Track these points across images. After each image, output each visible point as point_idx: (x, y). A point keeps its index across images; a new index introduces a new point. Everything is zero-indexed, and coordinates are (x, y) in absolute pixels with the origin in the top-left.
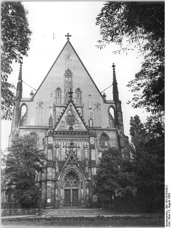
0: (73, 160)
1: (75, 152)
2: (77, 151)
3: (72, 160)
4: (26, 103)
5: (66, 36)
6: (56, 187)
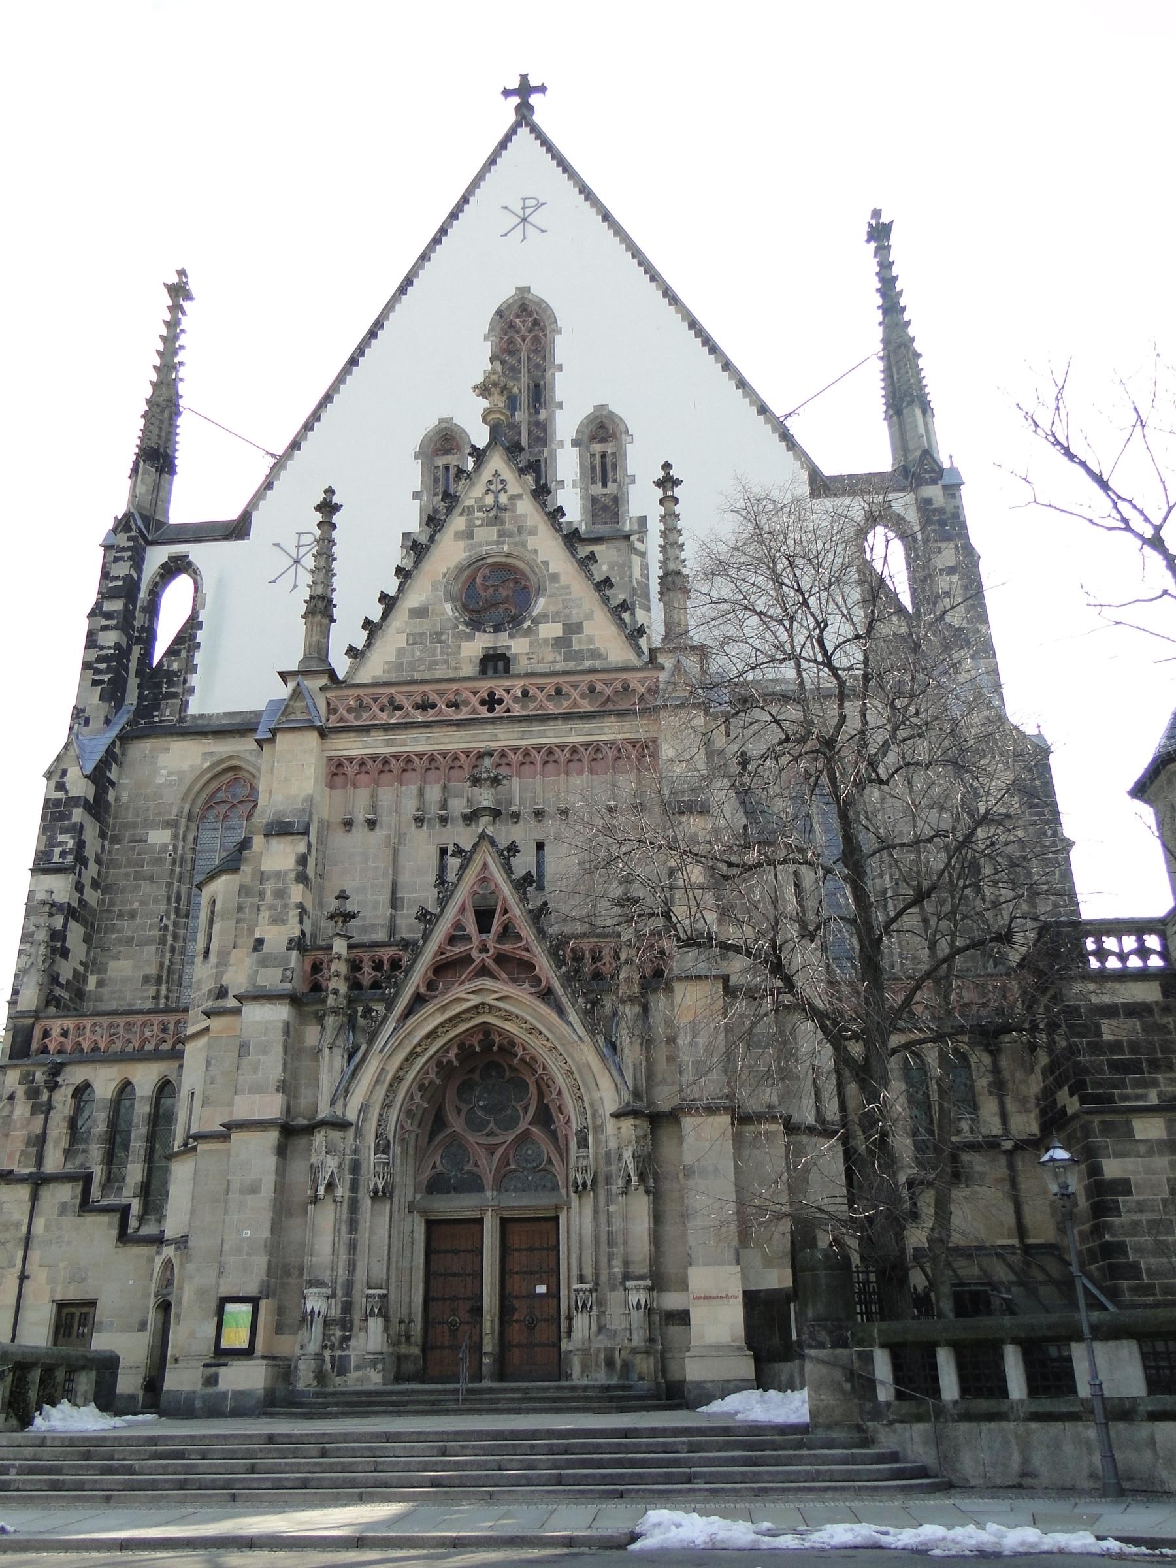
0: (496, 926)
1: (513, 849)
2: (548, 849)
4: (196, 552)
5: (507, 93)
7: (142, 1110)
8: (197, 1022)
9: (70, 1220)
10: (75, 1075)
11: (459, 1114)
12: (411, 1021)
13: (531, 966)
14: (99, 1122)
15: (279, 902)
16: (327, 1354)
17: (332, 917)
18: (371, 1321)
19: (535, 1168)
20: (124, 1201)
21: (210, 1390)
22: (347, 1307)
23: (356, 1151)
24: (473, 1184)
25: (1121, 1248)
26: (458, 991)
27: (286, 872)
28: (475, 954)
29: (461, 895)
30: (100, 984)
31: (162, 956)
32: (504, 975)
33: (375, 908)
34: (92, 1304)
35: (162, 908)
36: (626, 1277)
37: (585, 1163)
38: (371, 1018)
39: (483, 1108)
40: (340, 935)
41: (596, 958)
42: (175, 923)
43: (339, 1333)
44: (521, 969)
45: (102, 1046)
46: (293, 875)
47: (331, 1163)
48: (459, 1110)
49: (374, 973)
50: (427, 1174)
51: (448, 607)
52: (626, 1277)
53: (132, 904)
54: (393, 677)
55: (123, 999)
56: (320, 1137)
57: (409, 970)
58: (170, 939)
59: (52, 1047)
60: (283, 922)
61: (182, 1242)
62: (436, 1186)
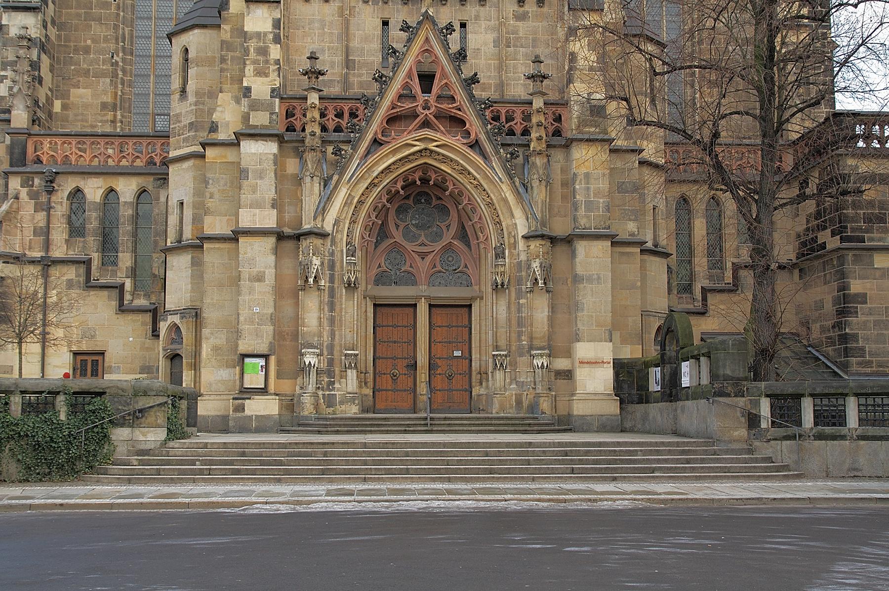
0: (435, 89)
1: (450, 28)
2: (469, 27)
3: (426, 89)
6: (306, 281)
7: (126, 212)
8: (180, 148)
9: (74, 293)
10: (67, 185)
11: (397, 229)
12: (371, 160)
13: (462, 123)
14: (93, 221)
15: (261, 58)
16: (320, 393)
17: (306, 73)
18: (349, 371)
19: (456, 270)
20: (119, 281)
21: (239, 415)
22: (331, 362)
23: (332, 254)
24: (410, 279)
25: (855, 337)
26: (407, 138)
27: (265, 34)
28: (420, 109)
29: (409, 62)
30: (65, 107)
31: (116, 87)
32: (442, 129)
33: (332, 67)
34: (102, 353)
35: (112, 46)
36: (531, 348)
37: (502, 270)
38: (341, 155)
39: (416, 226)
40: (314, 89)
41: (509, 119)
42: (124, 60)
43: (326, 379)
44: (456, 122)
45: (73, 158)
46: (271, 36)
47: (316, 261)
48: (397, 226)
49: (337, 120)
50: (375, 271)
52: (531, 348)
53: (85, 41)
55: (87, 121)
56: (305, 243)
57: (368, 121)
58: (120, 73)
59: (44, 159)
60: (267, 75)
62: (381, 279)
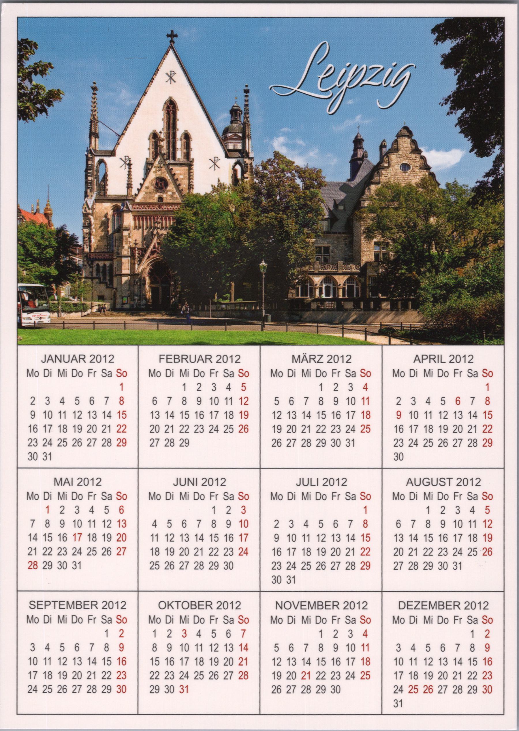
4: (106, 159)
7: (108, 268)
9: (98, 284)
22: (140, 298)
51: (152, 187)
54: (143, 201)
61: (116, 289)
